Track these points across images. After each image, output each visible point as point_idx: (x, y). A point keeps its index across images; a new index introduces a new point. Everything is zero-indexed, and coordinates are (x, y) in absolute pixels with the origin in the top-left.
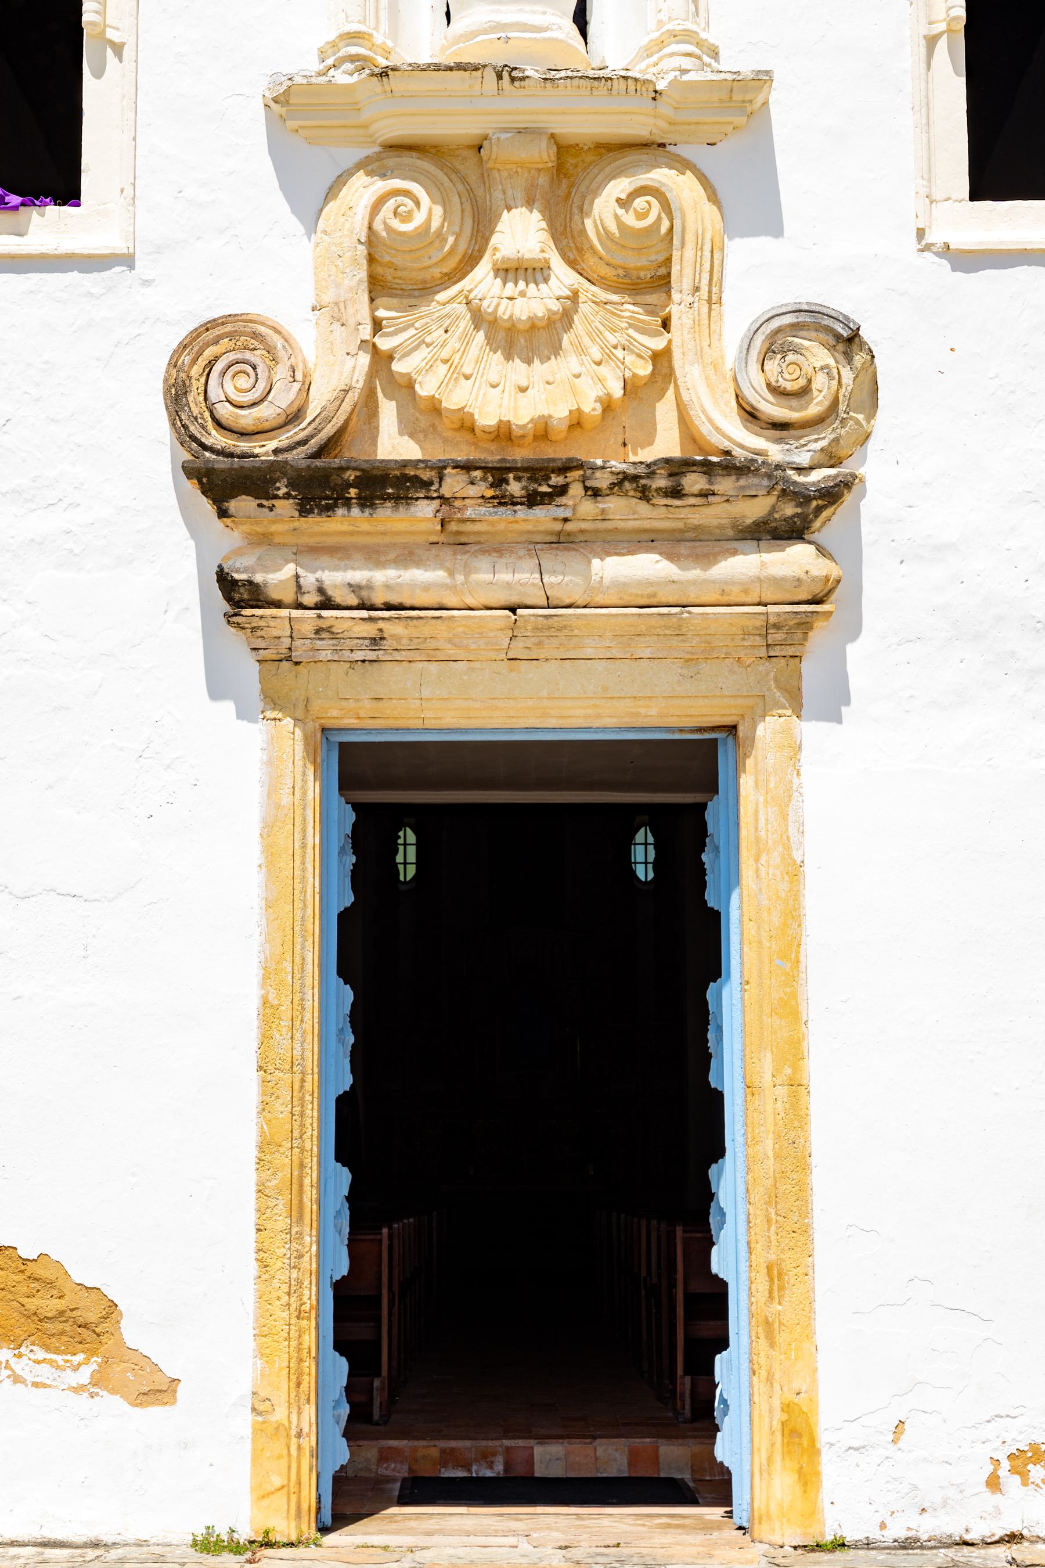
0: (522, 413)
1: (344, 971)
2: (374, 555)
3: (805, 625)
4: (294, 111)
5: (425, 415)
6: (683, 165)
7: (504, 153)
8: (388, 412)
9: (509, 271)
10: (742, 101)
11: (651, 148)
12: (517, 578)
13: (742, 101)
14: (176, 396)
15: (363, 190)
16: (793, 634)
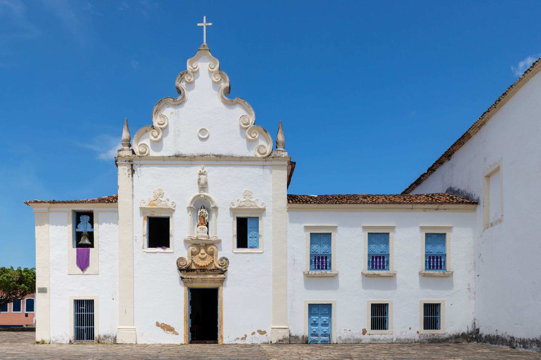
0: (203, 265)
1: (191, 305)
2: (192, 275)
3: (223, 281)
4: (186, 241)
5: (196, 265)
6: (215, 246)
7: (201, 244)
8: (193, 264)
9: (202, 254)
10: (219, 241)
11: (213, 244)
12: (202, 277)
13: (219, 241)
14: (177, 263)
15: (191, 248)
16: (222, 281)
